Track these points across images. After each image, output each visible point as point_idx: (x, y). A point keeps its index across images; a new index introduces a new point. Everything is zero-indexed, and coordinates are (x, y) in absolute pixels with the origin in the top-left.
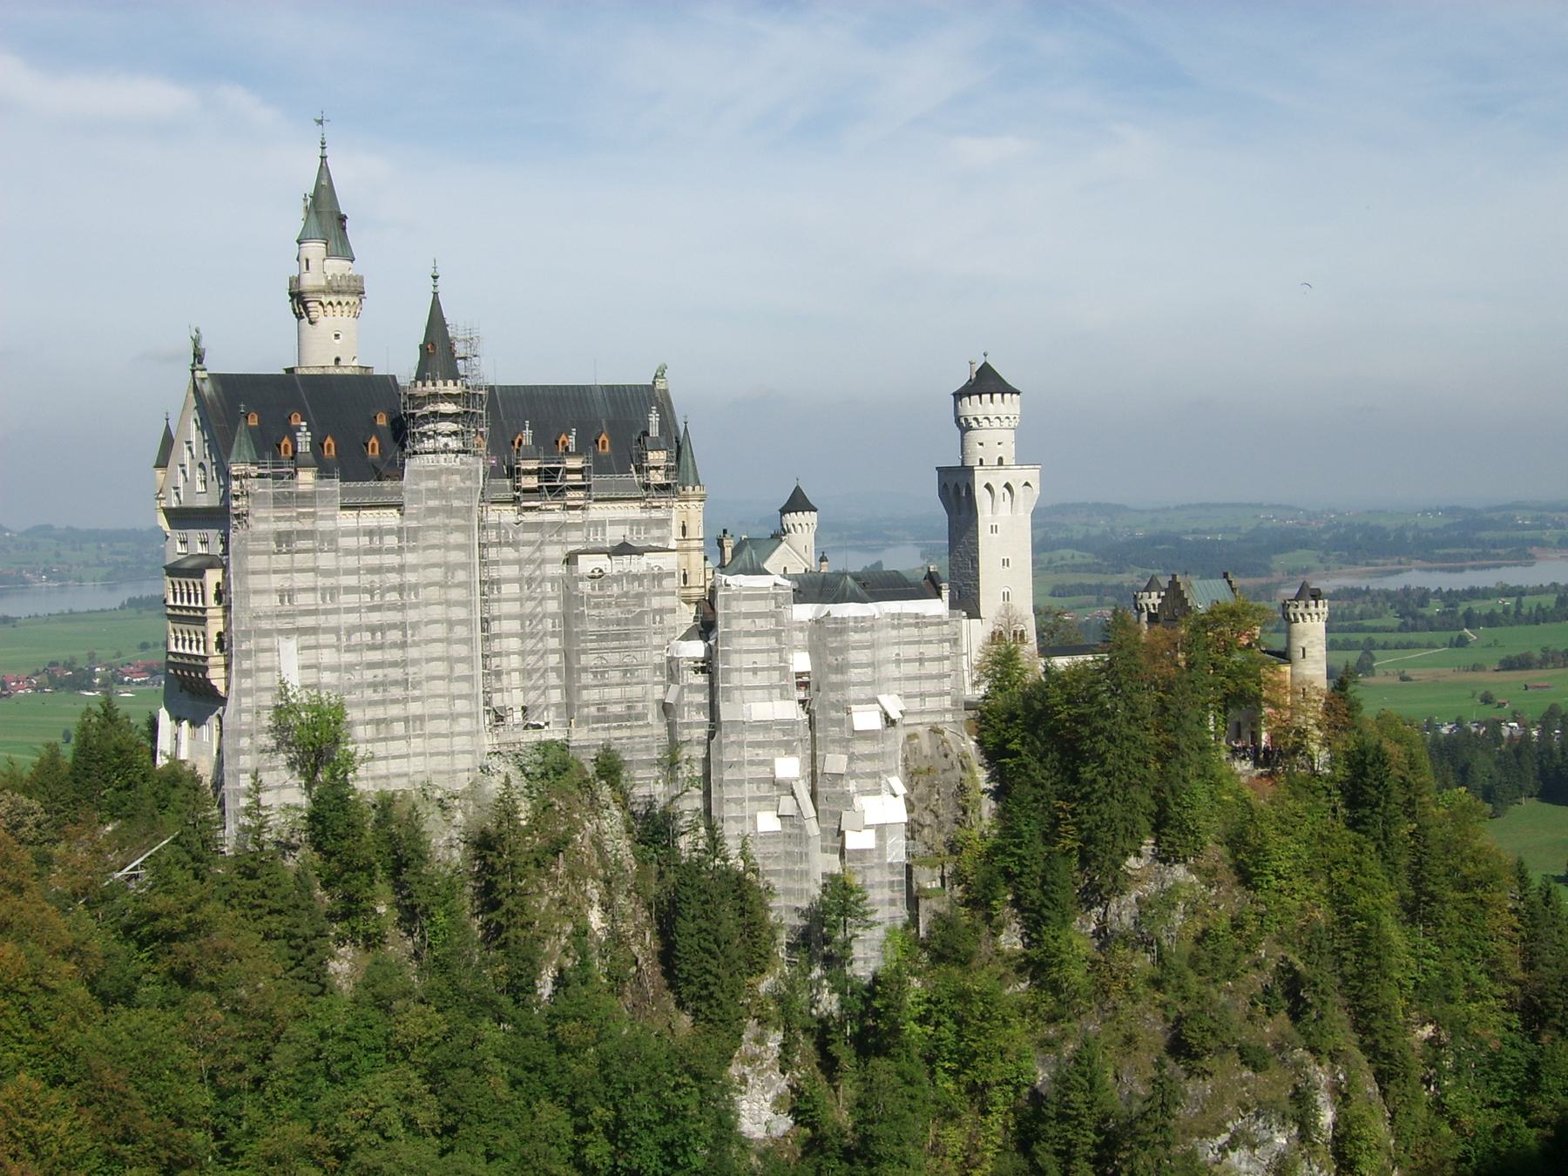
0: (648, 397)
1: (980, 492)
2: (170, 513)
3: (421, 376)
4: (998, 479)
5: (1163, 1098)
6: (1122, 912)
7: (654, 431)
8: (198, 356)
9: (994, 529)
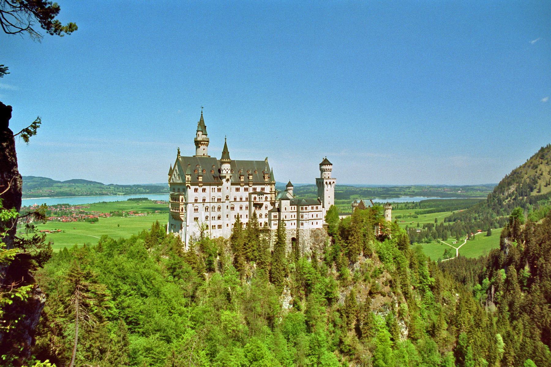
0: (264, 164)
1: (325, 183)
2: (170, 184)
3: (223, 158)
4: (328, 181)
5: (368, 302)
6: (357, 266)
7: (266, 170)
8: (179, 153)
9: (327, 190)
